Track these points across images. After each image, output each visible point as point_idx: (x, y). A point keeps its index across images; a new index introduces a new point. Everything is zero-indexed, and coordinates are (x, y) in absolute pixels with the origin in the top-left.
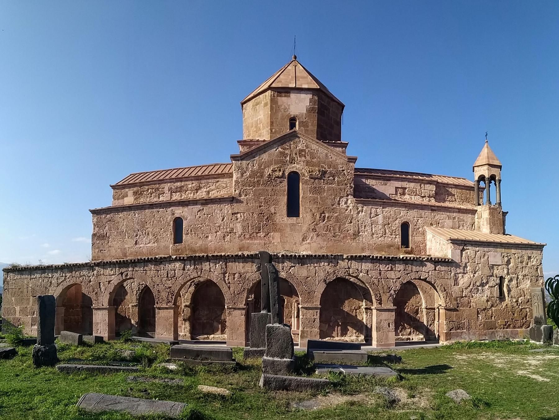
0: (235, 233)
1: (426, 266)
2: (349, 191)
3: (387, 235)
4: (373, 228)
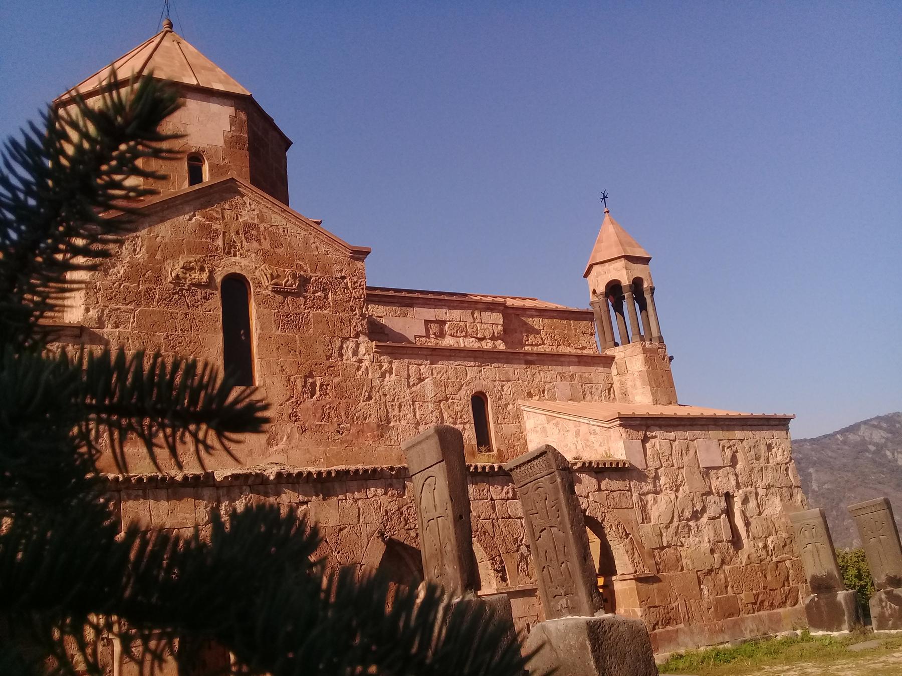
2: (359, 325)
4: (417, 409)
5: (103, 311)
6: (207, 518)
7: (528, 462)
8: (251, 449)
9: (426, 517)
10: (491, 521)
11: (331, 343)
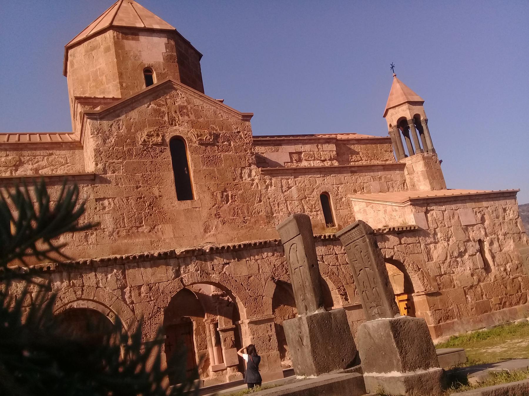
0: (104, 229)
1: (388, 240)
4: (289, 205)
5: (105, 164)
6: (174, 276)
7: (349, 231)
8: (196, 236)
9: (293, 267)
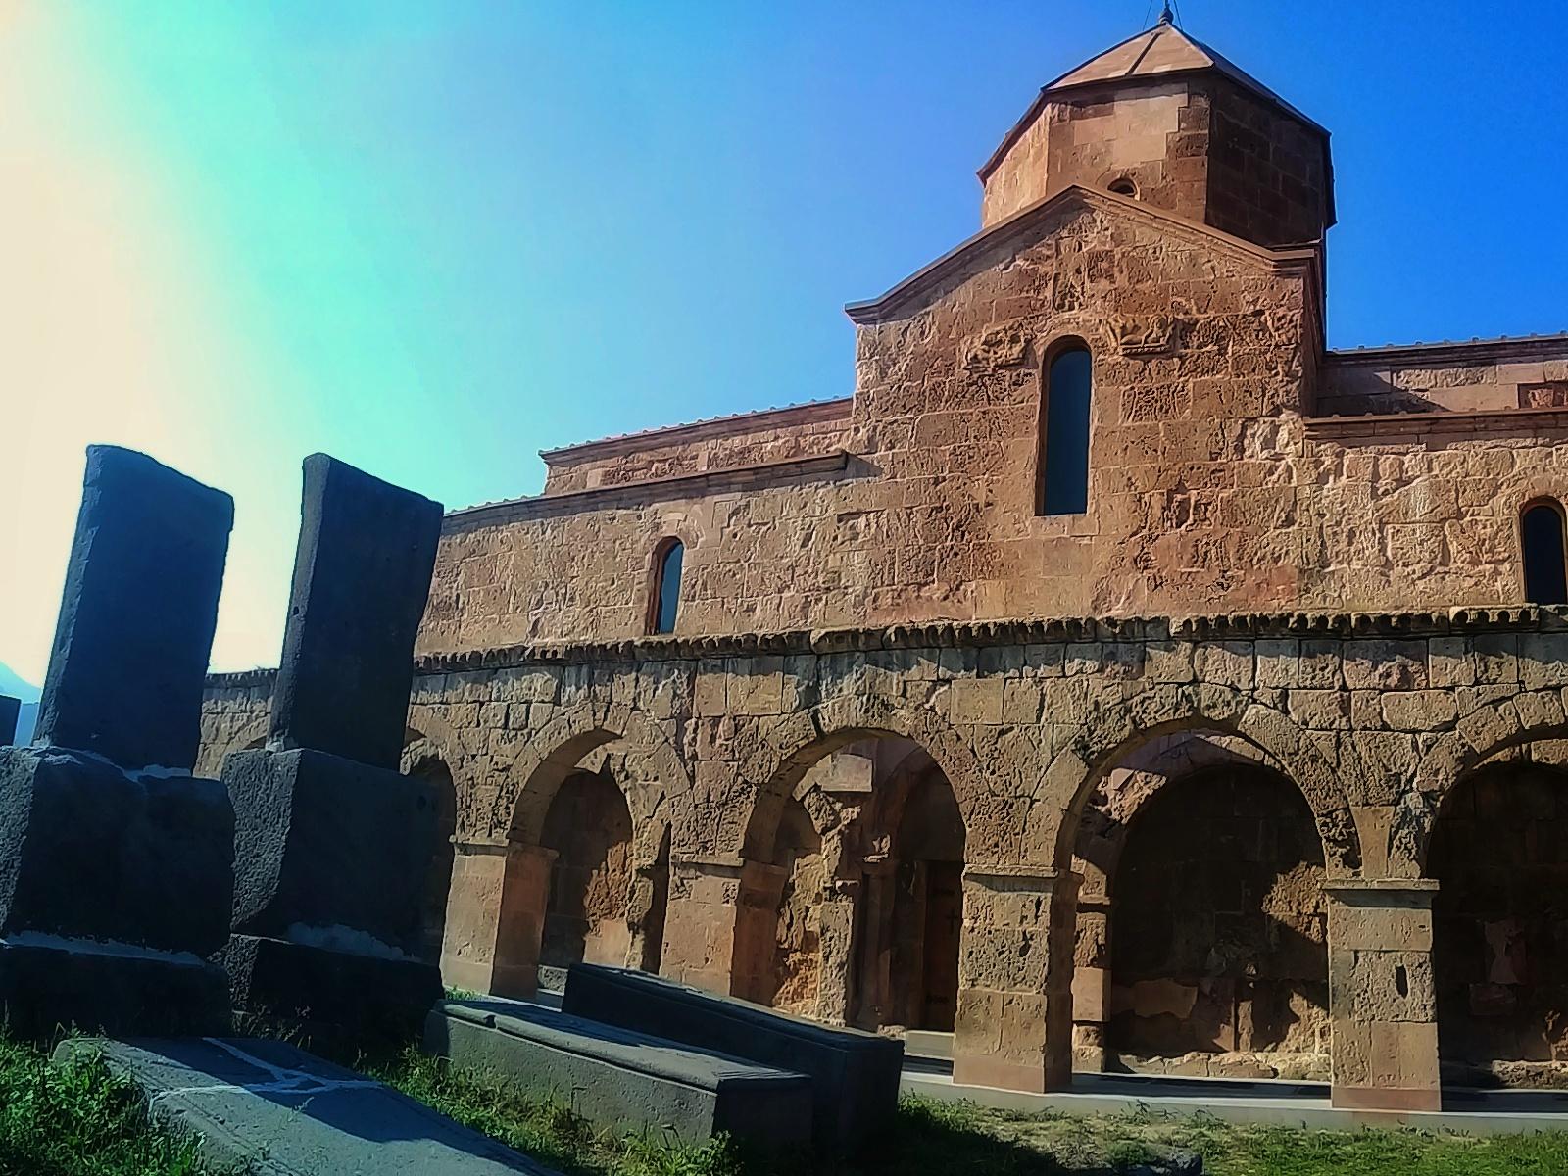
0: (846, 588)
3: (1453, 566)
10: (1333, 733)
11: (1223, 431)
